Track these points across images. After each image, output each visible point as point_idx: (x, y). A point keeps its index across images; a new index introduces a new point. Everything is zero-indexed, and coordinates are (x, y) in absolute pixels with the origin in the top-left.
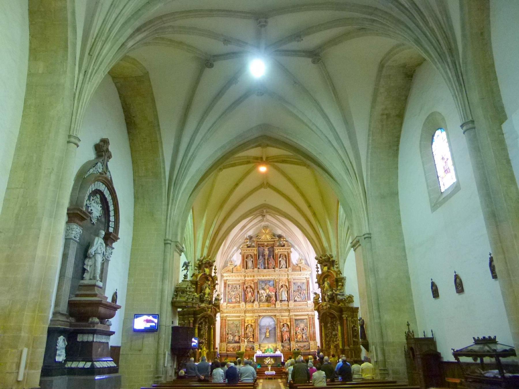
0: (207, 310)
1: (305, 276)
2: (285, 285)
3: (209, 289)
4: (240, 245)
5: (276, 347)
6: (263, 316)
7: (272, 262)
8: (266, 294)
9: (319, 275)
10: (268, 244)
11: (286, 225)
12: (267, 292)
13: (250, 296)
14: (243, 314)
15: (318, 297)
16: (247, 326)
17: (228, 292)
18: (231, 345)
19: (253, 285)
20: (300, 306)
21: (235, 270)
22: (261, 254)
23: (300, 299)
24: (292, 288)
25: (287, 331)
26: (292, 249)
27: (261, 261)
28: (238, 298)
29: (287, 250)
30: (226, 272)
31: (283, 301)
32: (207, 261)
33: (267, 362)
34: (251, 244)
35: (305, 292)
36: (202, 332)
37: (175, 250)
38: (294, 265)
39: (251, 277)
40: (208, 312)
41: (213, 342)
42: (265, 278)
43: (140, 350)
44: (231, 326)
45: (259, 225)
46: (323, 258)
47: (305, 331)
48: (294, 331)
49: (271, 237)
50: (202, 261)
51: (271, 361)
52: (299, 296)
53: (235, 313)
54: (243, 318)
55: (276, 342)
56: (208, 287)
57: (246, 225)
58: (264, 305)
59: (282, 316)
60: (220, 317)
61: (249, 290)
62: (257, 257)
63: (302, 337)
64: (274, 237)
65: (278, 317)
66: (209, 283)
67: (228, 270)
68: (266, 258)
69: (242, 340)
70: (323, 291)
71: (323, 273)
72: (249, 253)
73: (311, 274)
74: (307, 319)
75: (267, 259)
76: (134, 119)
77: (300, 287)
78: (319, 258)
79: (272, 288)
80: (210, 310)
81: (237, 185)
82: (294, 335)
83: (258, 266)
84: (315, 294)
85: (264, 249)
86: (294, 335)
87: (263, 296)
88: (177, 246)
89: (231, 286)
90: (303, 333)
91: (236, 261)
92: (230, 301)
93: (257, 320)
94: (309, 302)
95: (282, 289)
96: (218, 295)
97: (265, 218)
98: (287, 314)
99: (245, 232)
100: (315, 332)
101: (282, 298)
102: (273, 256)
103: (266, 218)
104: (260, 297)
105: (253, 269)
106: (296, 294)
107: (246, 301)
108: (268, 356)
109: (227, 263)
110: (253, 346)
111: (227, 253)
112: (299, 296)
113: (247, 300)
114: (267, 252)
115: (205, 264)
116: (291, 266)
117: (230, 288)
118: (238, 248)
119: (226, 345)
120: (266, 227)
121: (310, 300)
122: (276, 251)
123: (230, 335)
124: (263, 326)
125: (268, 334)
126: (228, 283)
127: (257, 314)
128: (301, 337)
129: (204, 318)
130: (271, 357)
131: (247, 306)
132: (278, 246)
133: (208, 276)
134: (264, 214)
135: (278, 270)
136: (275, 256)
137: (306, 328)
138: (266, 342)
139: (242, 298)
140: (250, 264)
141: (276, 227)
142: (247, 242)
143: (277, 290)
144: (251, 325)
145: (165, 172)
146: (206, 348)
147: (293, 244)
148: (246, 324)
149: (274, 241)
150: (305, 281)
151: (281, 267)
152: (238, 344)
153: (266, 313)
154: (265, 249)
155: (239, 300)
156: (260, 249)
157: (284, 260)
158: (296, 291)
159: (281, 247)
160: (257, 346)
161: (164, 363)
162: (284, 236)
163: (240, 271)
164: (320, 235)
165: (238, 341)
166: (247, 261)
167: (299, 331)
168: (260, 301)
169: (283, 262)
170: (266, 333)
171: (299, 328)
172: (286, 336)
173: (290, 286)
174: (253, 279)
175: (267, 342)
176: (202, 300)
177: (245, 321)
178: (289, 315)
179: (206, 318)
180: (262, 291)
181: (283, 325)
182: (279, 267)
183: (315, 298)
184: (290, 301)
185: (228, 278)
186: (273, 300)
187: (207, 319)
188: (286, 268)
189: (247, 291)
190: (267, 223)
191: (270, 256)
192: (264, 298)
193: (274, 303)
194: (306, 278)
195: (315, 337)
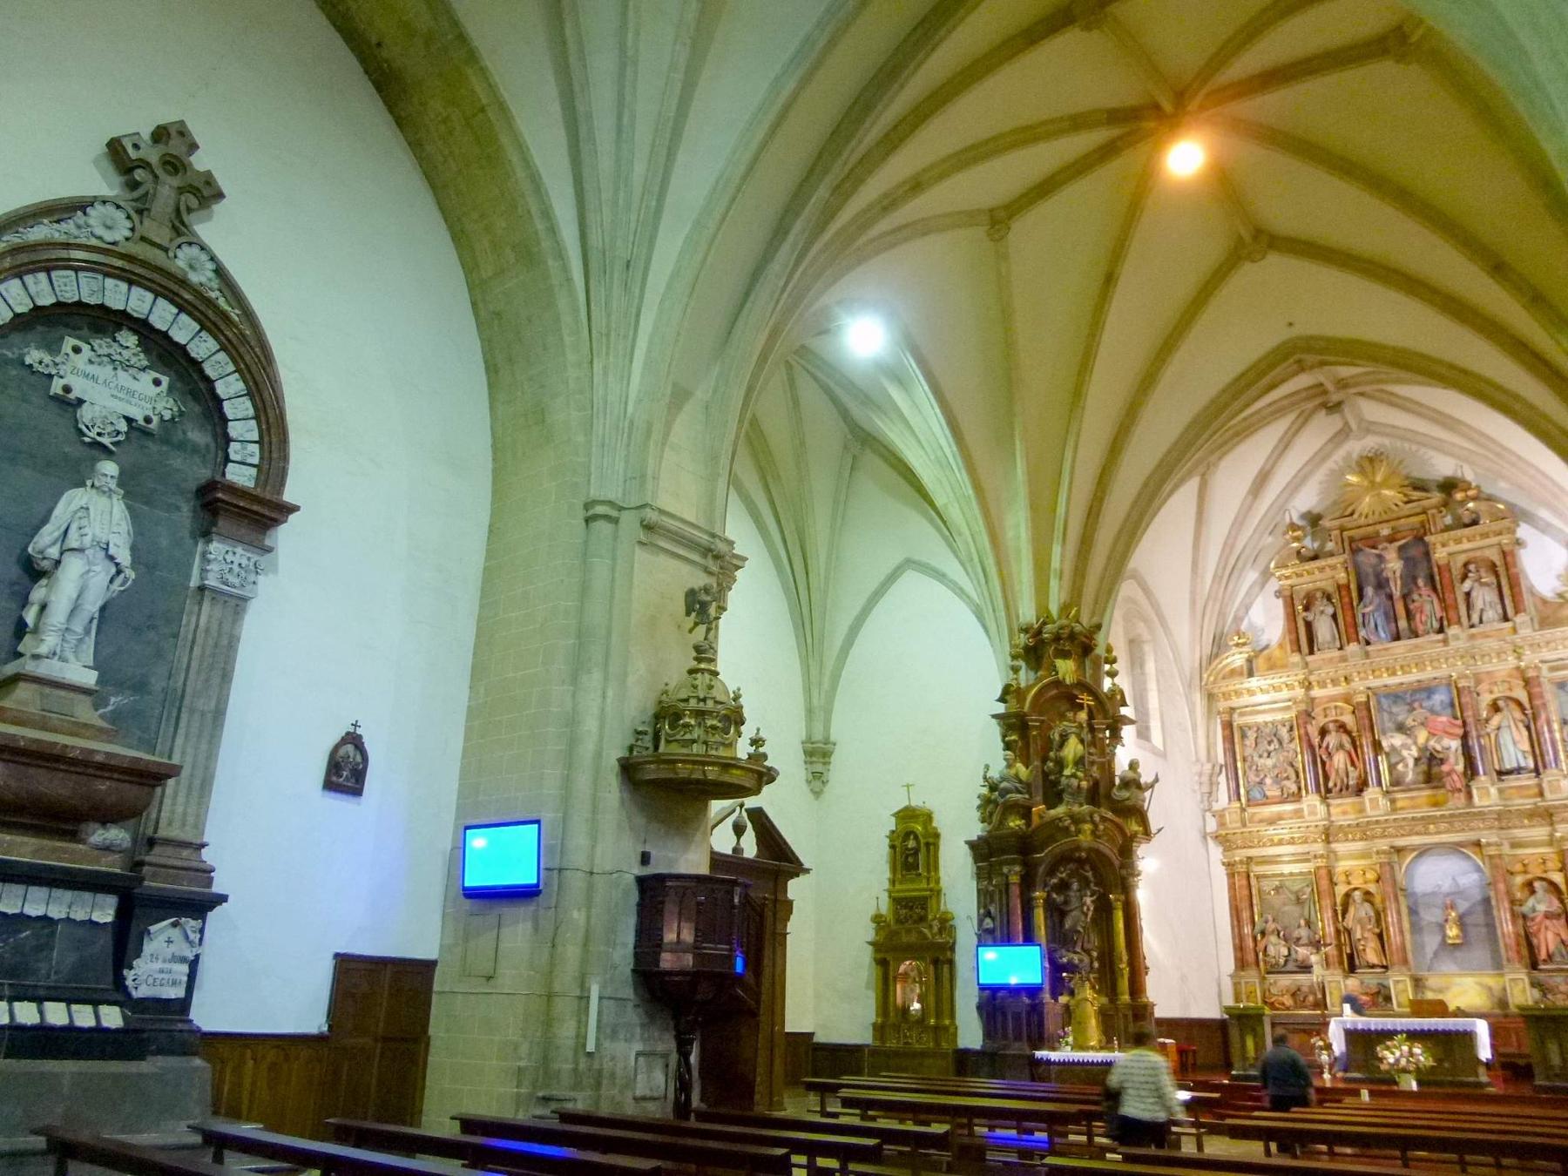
0: (1073, 828)
3: (1082, 741)
5: (1504, 989)
7: (1427, 605)
10: (1395, 531)
11: (1459, 422)
13: (1342, 766)
14: (1319, 848)
16: (1348, 895)
17: (1244, 760)
18: (1285, 981)
19: (1348, 719)
21: (1260, 663)
22: (1372, 579)
24: (1553, 707)
27: (1372, 605)
28: (1287, 778)
29: (1494, 540)
30: (1224, 678)
32: (1062, 628)
33: (1391, 1060)
34: (1322, 546)
36: (1068, 924)
37: (641, 543)
38: (1544, 602)
39: (1335, 682)
40: (1081, 837)
43: (489, 978)
44: (1275, 900)
49: (1405, 495)
50: (1039, 632)
51: (1411, 1054)
54: (1321, 862)
56: (1078, 736)
57: (1268, 467)
58: (1412, 798)
59: (1514, 845)
60: (1224, 864)
61: (1332, 739)
64: (1416, 495)
65: (1492, 851)
66: (1083, 716)
68: (1397, 593)
75: (1405, 597)
76: (385, 54)
80: (1087, 827)
81: (1110, 279)
83: (1362, 633)
87: (1403, 760)
88: (649, 527)
89: (1252, 735)
91: (1263, 630)
92: (1258, 796)
98: (1540, 832)
101: (1501, 760)
102: (1431, 579)
105: (1341, 648)
108: (1402, 1032)
110: (1385, 983)
113: (1331, 784)
114: (1394, 565)
115: (1057, 638)
117: (1250, 741)
118: (1266, 575)
120: (1369, 462)
122: (1440, 555)
123: (1273, 939)
124: (1425, 895)
125: (1453, 931)
127: (1383, 845)
129: (1072, 866)
130: (1414, 1036)
132: (1447, 529)
133: (1076, 692)
134: (1335, 398)
136: (1437, 578)
138: (1447, 966)
140: (1324, 630)
141: (1423, 450)
144: (1367, 893)
145: (553, 230)
146: (1093, 988)
147: (1522, 502)
148: (1341, 890)
149: (1424, 512)
153: (1427, 833)
155: (1294, 788)
156: (1361, 558)
157: (1486, 584)
160: (1400, 986)
161: (581, 1038)
162: (1469, 476)
169: (1484, 597)
170: (1442, 927)
172: (1550, 936)
173: (1537, 702)
175: (1453, 968)
176: (1054, 794)
178: (1551, 835)
179: (1080, 862)
180: (1398, 740)
181: (1529, 887)
182: (1464, 619)
184: (1548, 771)
186: (1449, 774)
187: (1087, 867)
188: (1506, 618)
189: (1327, 747)
190: (1370, 442)
191: (1414, 579)
192: (1410, 773)
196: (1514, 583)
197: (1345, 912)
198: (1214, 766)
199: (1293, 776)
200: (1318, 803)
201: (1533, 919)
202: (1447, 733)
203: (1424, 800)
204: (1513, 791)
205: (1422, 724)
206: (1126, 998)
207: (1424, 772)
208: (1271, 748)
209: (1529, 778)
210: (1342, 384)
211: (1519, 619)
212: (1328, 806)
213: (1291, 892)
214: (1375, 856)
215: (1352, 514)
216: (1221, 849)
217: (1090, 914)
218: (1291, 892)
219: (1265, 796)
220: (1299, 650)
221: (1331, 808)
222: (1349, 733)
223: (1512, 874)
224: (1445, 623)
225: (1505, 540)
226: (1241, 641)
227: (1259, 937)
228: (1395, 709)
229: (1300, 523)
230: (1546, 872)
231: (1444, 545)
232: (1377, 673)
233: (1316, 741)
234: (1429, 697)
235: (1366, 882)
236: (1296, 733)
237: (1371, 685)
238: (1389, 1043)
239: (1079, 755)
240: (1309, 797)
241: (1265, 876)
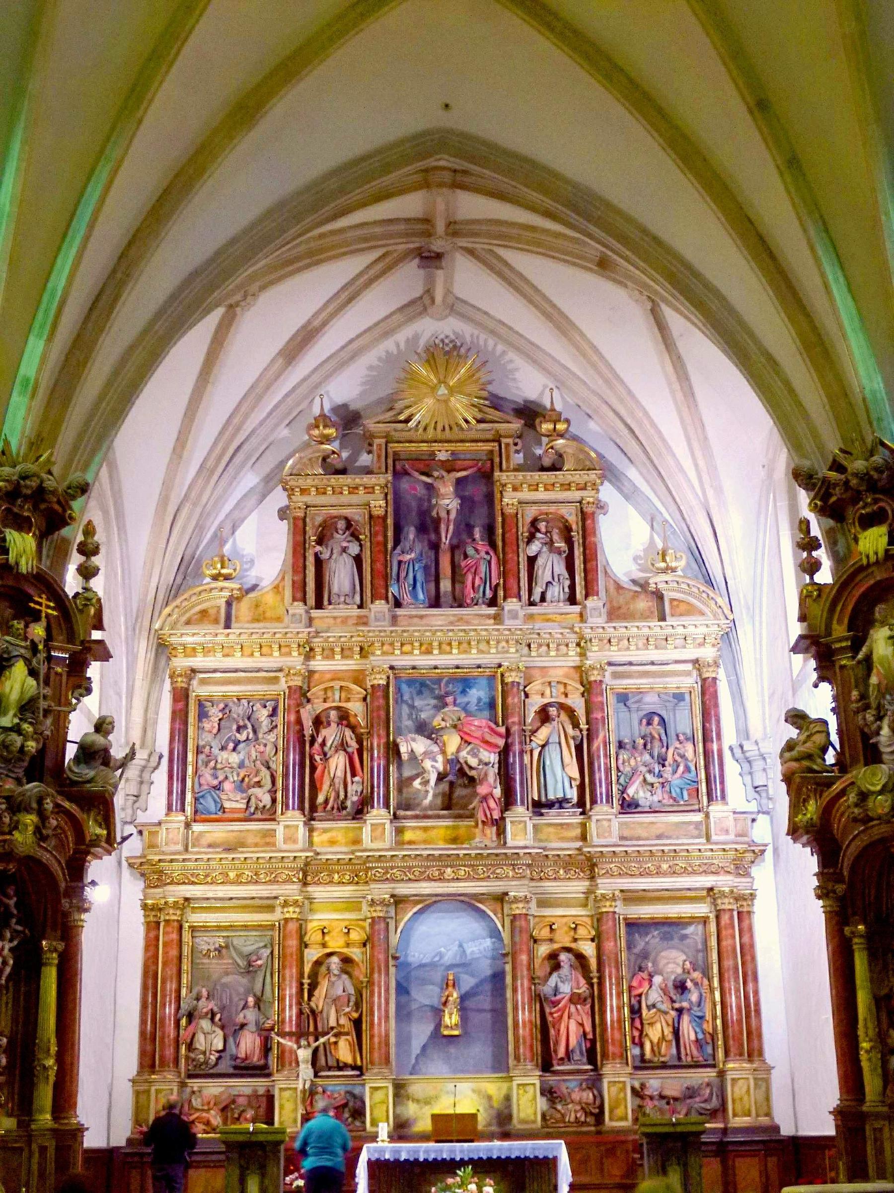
0: (7, 820)
1: (691, 653)
2: (562, 707)
3: (33, 673)
4: (283, 463)
5: (508, 1098)
6: (419, 899)
8: (440, 758)
9: (820, 588)
12: (451, 748)
13: (340, 773)
14: (292, 890)
15: (819, 739)
16: (318, 963)
17: (198, 751)
18: (213, 1089)
19: (356, 708)
20: (659, 837)
21: (243, 609)
22: (414, 516)
23: (656, 798)
25: (575, 999)
26: (607, 492)
28: (258, 784)
29: (576, 495)
30: (188, 623)
31: (550, 805)
32: (24, 477)
34: (354, 457)
35: (690, 754)
38: (619, 587)
39: (345, 653)
40: (17, 834)
41: (50, 1062)
42: (437, 659)
44: (215, 967)
45: (402, 336)
46: (859, 465)
47: (694, 997)
48: (620, 994)
52: (650, 778)
53: (237, 882)
54: (291, 912)
55: (508, 1070)
56: (27, 662)
57: (316, 323)
58: (425, 829)
59: (543, 903)
60: (145, 907)
61: (330, 734)
62: (390, 534)
63: (676, 1033)
64: (493, 414)
65: (518, 909)
66: (38, 631)
67: (204, 613)
69: (281, 1058)
70: (855, 694)
71: (844, 584)
72: (334, 512)
73: (728, 637)
74: (705, 921)
75: (453, 548)
77: (656, 719)
78: (824, 471)
79: (480, 723)
80: (30, 819)
82: (620, 1021)
83: (393, 589)
84: (797, 718)
85: (429, 487)
86: (620, 1021)
87: (422, 772)
89: (215, 713)
90: (680, 1011)
91: (252, 562)
92: (212, 807)
93: (383, 925)
94: (716, 810)
95: (543, 733)
96: (102, 726)
97: (440, 275)
98: (577, 887)
99: (315, 378)
100: (757, 1003)
102: (490, 530)
103: (448, 292)
104: (404, 783)
105: (361, 606)
106: (630, 761)
107: (313, 808)
108: (462, 1163)
109: (199, 575)
110: (357, 1091)
111: (195, 505)
112: (650, 778)
113: (321, 799)
116: (602, 593)
117: (211, 724)
119: (175, 1089)
121: (723, 797)
122: (509, 499)
123: (205, 1024)
124: (422, 966)
125: (451, 1018)
126: (199, 690)
127: (381, 891)
128: (670, 1036)
131: (316, 838)
133: (31, 591)
134: (437, 245)
135: (521, 614)
137: (696, 975)
138: (437, 1066)
139: (285, 789)
141: (511, 355)
142: (327, 439)
143: (516, 739)
144: (347, 960)
147: (613, 456)
148: (312, 954)
150: (689, 682)
151: (536, 597)
152: (259, 1084)
154: (438, 485)
155: (266, 800)
156: (405, 484)
158: (634, 747)
159: (537, 476)
160: (379, 1095)
162: (558, 407)
163: (279, 619)
164: (828, 324)
165: (256, 1059)
166: (325, 556)
167: (654, 996)
168: (406, 805)
170: (438, 1012)
171: (657, 980)
173: (598, 715)
174: (362, 671)
177: (301, 934)
178: (589, 892)
180: (420, 745)
181: (553, 957)
183: (800, 749)
184: (597, 808)
185: (198, 662)
186: (485, 798)
189: (323, 744)
191: (469, 528)
193: (496, 815)
194: (696, 662)
195: (754, 1035)
196: (590, 554)
197: (313, 986)
198: (150, 755)
199: (268, 785)
200: (301, 824)
201: (555, 1004)
202: (487, 743)
203: (442, 832)
204: (551, 829)
205: (455, 727)
206: (45, 1118)
207: (444, 794)
208: (242, 737)
209: (574, 814)
210: (455, 229)
211: (591, 602)
212: (311, 830)
213: (240, 954)
214: (365, 907)
215: (407, 421)
216: (141, 884)
217: (8, 970)
218: (240, 954)
219: (223, 809)
220: (304, 600)
221: (315, 834)
222: (353, 728)
223: (535, 941)
224: (501, 593)
225: (588, 495)
226: (224, 571)
227: (184, 1022)
228: (418, 703)
229: (334, 418)
230: (575, 940)
231: (515, 489)
232: (407, 648)
233: (308, 731)
234: (464, 692)
235: (348, 945)
236: (279, 720)
237: (394, 663)
238: (450, 1181)
239: (27, 696)
240: (290, 813)
241: (205, 929)
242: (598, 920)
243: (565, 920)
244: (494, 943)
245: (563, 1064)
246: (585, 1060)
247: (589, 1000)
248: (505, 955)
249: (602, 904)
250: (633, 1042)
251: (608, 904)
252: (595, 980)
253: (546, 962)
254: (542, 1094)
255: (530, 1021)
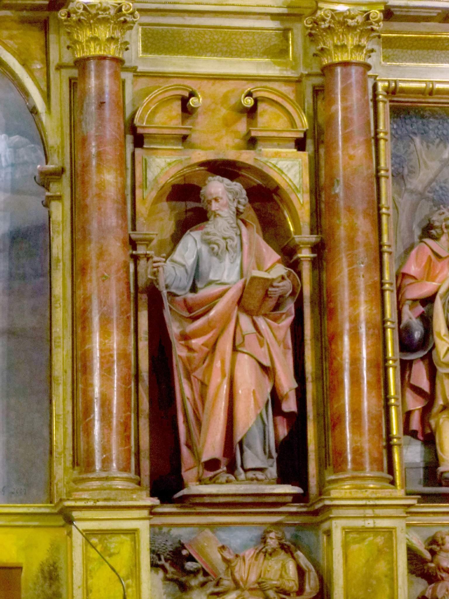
242: (317, 91)
243: (222, 88)
244: (15, 148)
245: (213, 480)
246: (273, 471)
247: (290, 306)
248: (58, 174)
249: (329, 42)
250: (407, 431)
251: (351, 41)
252: (305, 254)
253: (165, 205)
254: (154, 565)
255: (123, 356)
